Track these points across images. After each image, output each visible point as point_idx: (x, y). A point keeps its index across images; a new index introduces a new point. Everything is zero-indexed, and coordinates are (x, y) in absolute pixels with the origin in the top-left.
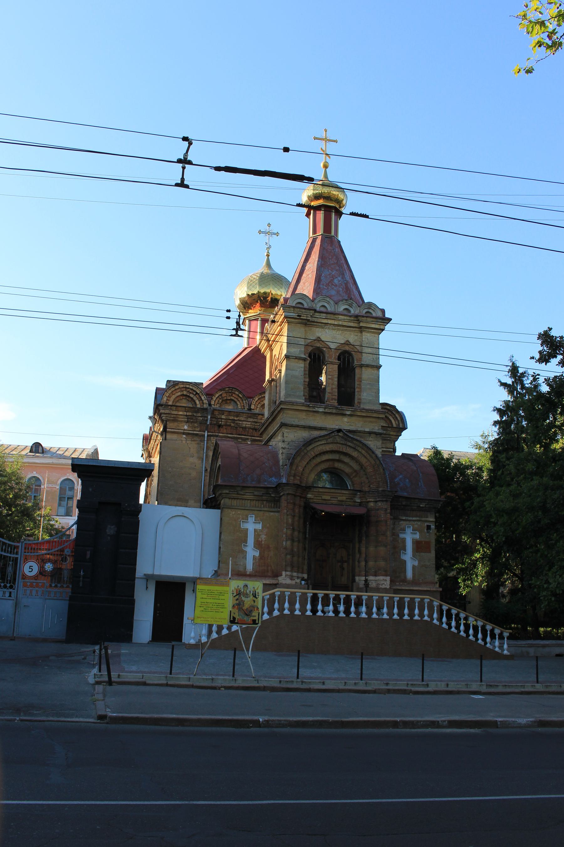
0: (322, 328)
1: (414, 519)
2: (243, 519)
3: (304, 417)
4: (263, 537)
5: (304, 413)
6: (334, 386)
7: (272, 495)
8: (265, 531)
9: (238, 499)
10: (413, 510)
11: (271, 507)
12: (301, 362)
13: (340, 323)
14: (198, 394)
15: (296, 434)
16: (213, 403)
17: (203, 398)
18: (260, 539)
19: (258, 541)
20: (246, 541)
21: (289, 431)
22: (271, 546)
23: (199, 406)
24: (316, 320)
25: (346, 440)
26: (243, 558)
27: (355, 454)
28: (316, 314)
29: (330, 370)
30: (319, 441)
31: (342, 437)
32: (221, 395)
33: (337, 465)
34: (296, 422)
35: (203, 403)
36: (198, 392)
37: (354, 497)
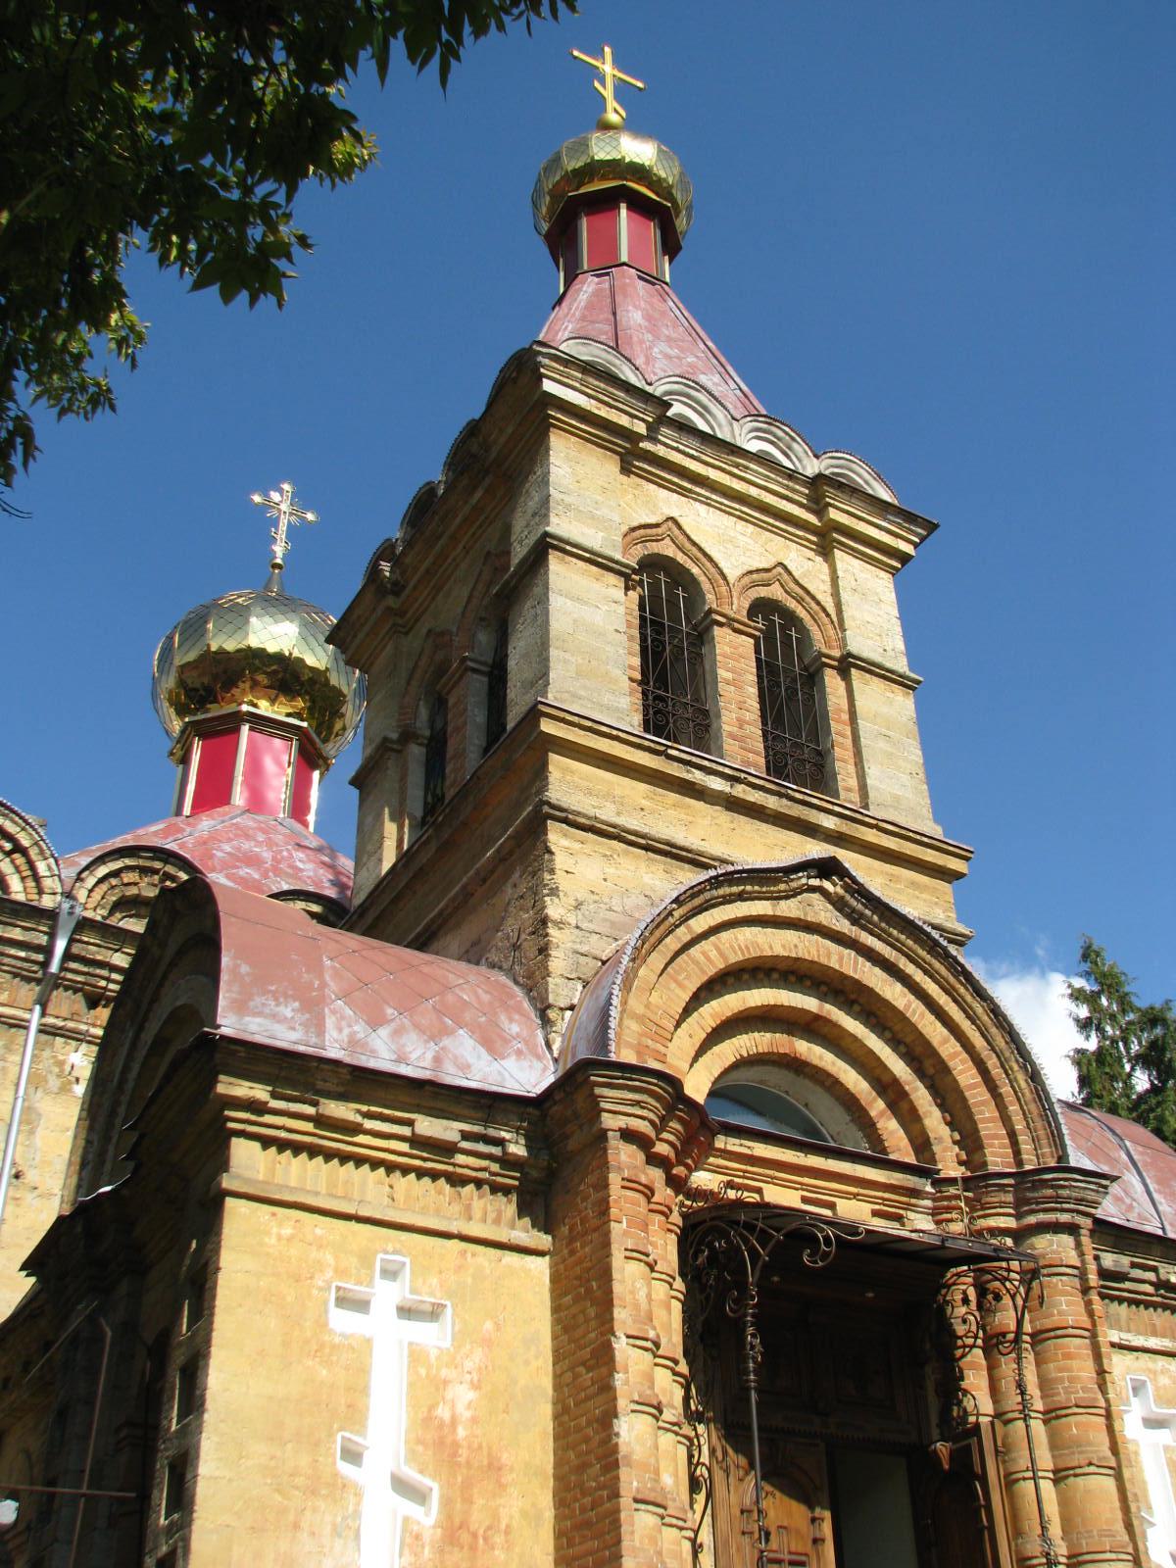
0: (683, 492)
1: (1153, 1343)
2: (341, 1273)
3: (645, 803)
4: (462, 1396)
5: (642, 787)
6: (748, 716)
7: (513, 1149)
8: (475, 1359)
9: (313, 1151)
10: (1137, 1303)
11: (497, 1221)
12: (612, 578)
13: (754, 492)
14: (24, 851)
15: (611, 870)
16: (82, 895)
17: (42, 867)
18: (443, 1412)
19: (428, 1420)
20: (355, 1414)
21: (577, 846)
22: (505, 1457)
23: (21, 897)
24: (661, 451)
25: (855, 919)
26: (336, 1532)
27: (894, 993)
28: (663, 429)
29: (727, 649)
30: (741, 897)
31: (838, 904)
32: (116, 874)
33: (804, 1048)
34: (607, 813)
35: (41, 892)
36: (25, 842)
37: (909, 1207)
